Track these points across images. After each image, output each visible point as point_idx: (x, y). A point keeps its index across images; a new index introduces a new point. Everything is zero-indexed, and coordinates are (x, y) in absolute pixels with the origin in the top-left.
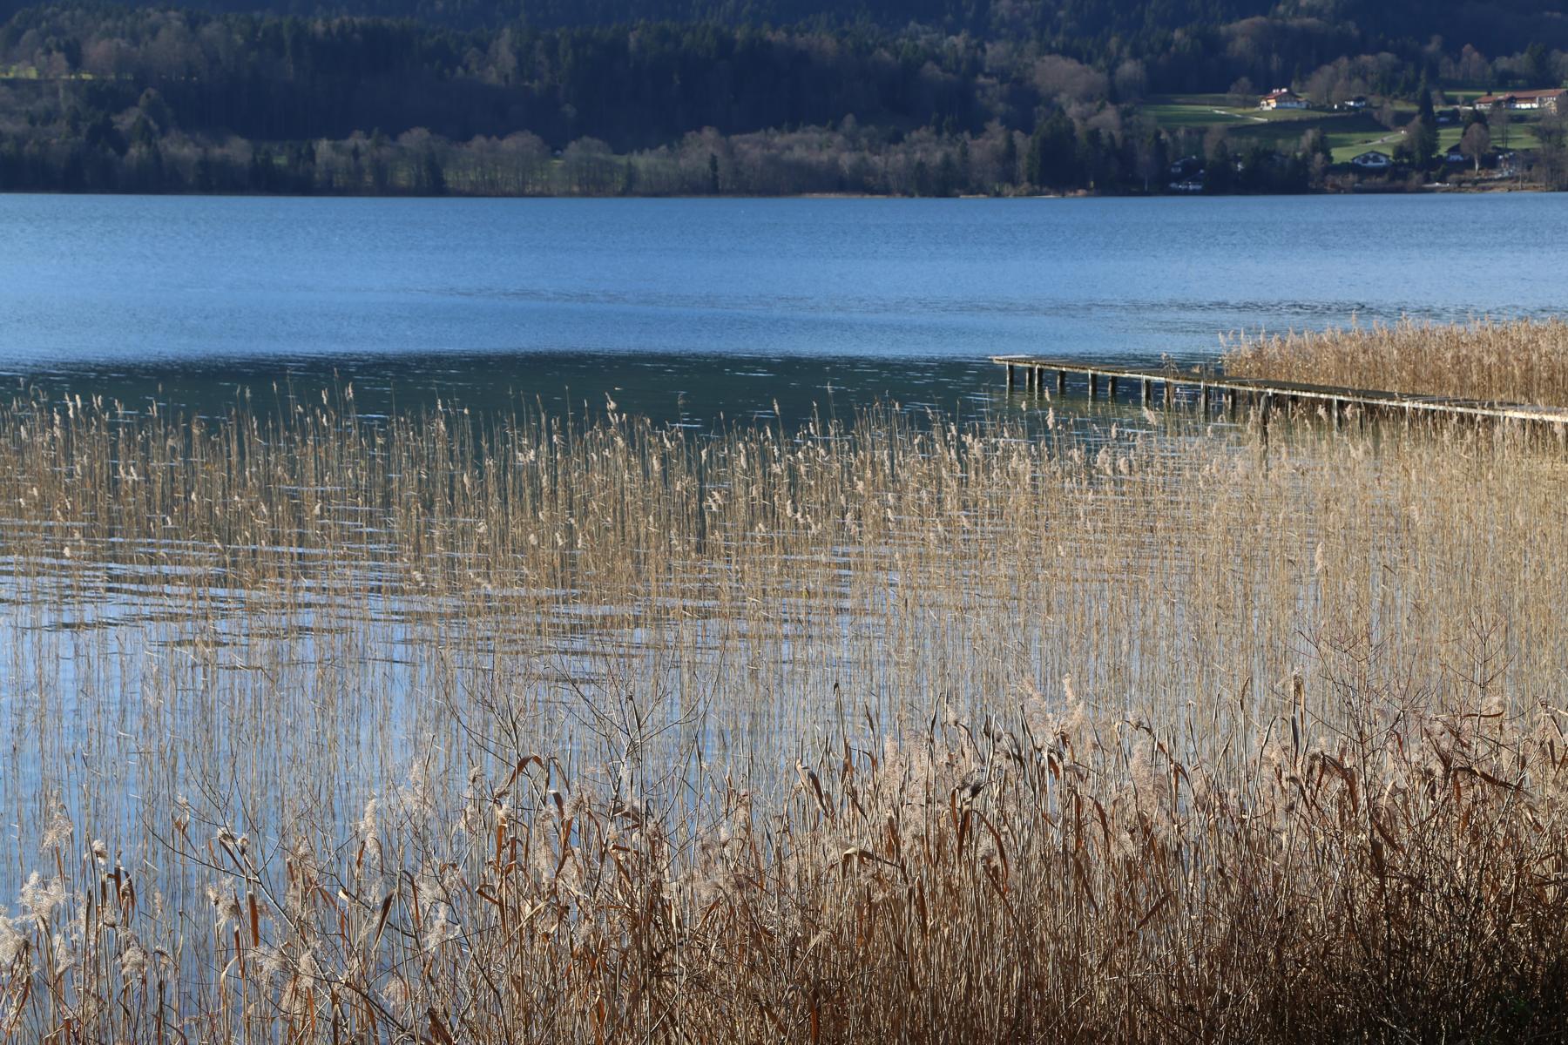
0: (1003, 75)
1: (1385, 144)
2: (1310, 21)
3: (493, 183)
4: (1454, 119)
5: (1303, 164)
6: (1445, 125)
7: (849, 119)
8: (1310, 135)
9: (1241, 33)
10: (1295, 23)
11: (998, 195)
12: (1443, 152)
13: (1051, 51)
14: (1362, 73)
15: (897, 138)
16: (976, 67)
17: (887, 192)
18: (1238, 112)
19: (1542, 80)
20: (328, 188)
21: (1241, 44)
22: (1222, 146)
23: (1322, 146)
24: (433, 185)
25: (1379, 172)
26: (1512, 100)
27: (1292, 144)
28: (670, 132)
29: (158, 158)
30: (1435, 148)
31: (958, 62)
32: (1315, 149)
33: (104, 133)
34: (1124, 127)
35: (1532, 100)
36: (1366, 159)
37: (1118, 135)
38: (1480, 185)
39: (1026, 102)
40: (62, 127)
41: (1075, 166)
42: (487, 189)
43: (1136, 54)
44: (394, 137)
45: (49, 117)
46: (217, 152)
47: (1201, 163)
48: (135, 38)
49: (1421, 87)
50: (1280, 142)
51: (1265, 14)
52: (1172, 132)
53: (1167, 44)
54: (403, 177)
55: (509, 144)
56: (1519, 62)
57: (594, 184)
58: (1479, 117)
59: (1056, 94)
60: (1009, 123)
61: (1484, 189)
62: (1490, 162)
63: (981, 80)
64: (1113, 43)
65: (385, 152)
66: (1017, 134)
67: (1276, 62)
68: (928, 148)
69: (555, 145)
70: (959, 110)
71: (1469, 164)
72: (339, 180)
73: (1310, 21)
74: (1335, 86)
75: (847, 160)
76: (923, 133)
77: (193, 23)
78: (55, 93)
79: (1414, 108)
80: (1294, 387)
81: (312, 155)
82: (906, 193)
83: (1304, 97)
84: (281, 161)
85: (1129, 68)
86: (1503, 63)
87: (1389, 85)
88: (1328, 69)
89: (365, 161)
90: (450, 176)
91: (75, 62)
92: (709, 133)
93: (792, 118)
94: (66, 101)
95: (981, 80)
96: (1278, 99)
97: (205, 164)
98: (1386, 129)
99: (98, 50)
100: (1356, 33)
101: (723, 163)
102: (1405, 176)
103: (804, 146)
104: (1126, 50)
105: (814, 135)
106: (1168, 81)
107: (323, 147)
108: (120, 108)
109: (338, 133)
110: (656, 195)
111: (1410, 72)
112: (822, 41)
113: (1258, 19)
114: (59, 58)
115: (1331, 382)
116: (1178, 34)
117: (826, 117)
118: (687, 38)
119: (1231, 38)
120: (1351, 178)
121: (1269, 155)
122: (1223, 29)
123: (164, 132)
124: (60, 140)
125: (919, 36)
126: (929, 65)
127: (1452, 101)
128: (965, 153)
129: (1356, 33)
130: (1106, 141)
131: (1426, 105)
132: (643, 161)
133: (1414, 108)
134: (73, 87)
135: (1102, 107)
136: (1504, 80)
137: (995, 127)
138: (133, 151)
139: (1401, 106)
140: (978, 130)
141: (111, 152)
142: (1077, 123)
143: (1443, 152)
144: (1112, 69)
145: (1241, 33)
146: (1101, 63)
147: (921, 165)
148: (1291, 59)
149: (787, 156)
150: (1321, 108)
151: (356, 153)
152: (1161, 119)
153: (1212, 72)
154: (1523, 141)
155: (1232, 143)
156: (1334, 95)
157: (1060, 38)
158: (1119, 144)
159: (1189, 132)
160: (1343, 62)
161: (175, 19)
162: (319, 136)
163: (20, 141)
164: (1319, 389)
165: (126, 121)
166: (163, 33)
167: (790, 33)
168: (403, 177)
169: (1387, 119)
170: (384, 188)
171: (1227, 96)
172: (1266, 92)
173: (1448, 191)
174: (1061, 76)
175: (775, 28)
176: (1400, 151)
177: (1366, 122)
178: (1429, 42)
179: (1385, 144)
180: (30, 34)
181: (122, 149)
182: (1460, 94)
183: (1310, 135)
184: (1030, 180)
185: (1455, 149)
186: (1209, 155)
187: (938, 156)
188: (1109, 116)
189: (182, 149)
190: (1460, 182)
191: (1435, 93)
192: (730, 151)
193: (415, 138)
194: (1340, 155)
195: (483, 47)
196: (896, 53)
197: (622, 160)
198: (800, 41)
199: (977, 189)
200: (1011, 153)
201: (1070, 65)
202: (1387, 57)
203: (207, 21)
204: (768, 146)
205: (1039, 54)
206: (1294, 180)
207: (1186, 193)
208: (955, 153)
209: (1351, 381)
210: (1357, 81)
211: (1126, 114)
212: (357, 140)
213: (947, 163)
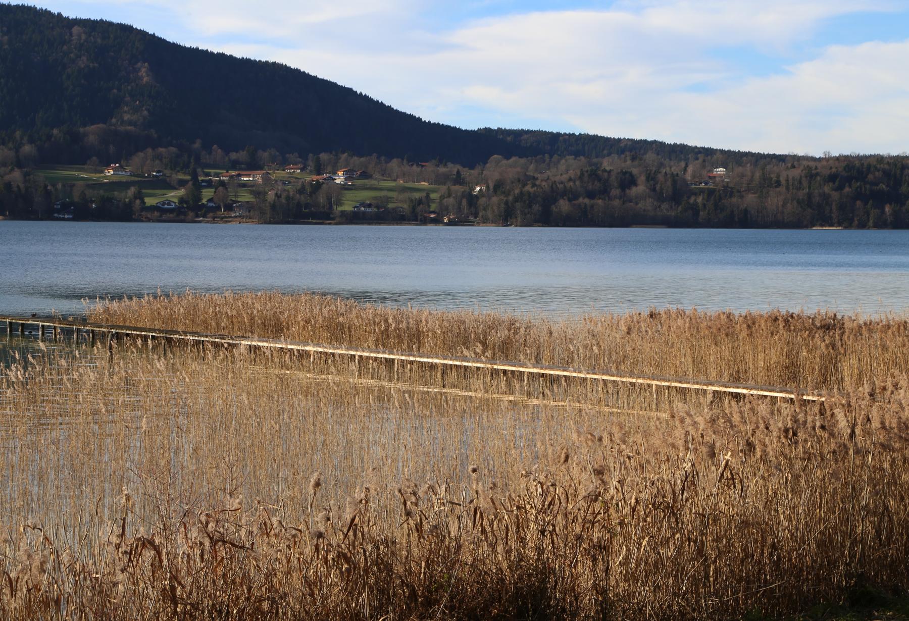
1: (174, 196)
2: (129, 128)
4: (209, 184)
5: (129, 206)
8: (132, 190)
9: (92, 132)
10: (122, 128)
12: (204, 201)
14: (159, 157)
18: (94, 176)
19: (253, 165)
21: (92, 139)
23: (140, 196)
25: (171, 211)
26: (239, 175)
27: (123, 195)
30: (200, 199)
32: (136, 198)
38: (225, 220)
43: (31, 141)
49: (192, 166)
50: (116, 193)
51: (105, 123)
52: (54, 185)
56: (241, 155)
58: (222, 183)
62: (229, 208)
64: (18, 134)
67: (112, 148)
71: (218, 208)
73: (129, 128)
74: (145, 163)
79: (188, 177)
83: (128, 169)
85: (27, 149)
86: (234, 156)
87: (174, 165)
88: (141, 154)
96: (114, 169)
98: (173, 188)
102: (185, 214)
104: (26, 139)
106: (51, 157)
113: (101, 125)
116: (55, 131)
120: (156, 214)
122: (81, 130)
127: (208, 175)
130: (15, 189)
131: (195, 176)
133: (188, 177)
135: (12, 170)
136: (234, 165)
139: (181, 176)
143: (204, 201)
144: (17, 149)
145: (92, 132)
146: (10, 145)
148: (120, 148)
150: (138, 176)
153: (77, 154)
154: (245, 197)
155: (89, 193)
158: (23, 191)
159: (64, 186)
160: (149, 150)
172: (107, 165)
176: (182, 200)
177: (165, 184)
178: (195, 143)
179: (174, 196)
182: (212, 171)
183: (132, 190)
185: (210, 200)
186: (76, 199)
188: (16, 176)
191: (199, 170)
194: (150, 201)
202: (173, 149)
206: (124, 213)
207: (64, 219)
210: (157, 162)
211: (26, 175)
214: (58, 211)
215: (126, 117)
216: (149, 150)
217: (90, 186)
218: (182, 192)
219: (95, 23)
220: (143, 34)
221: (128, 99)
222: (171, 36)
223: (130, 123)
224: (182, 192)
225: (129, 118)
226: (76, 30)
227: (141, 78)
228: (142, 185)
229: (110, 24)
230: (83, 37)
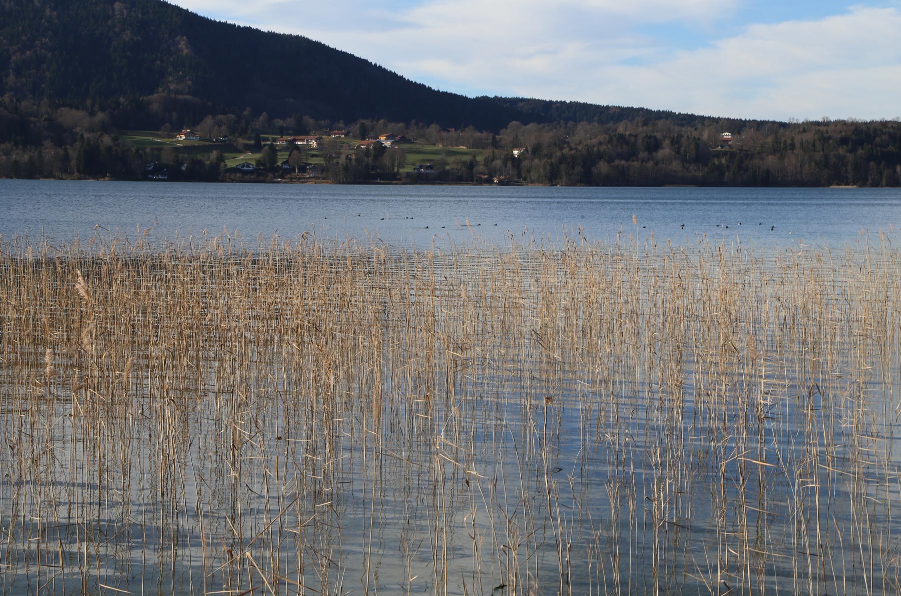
23: (221, 159)
25: (251, 172)
35: (303, 140)
36: (243, 166)
39: (61, 135)
61: (303, 182)
62: (303, 169)
96: (186, 134)
120: (239, 175)
128: (40, 156)
147: (16, 162)
159: (152, 149)
171: (159, 133)
172: (180, 132)
173: (286, 182)
176: (259, 163)
184: (79, 171)
187: (26, 157)
190: (292, 178)
194: (230, 164)
199: (49, 175)
207: (159, 180)
221: (170, 69)
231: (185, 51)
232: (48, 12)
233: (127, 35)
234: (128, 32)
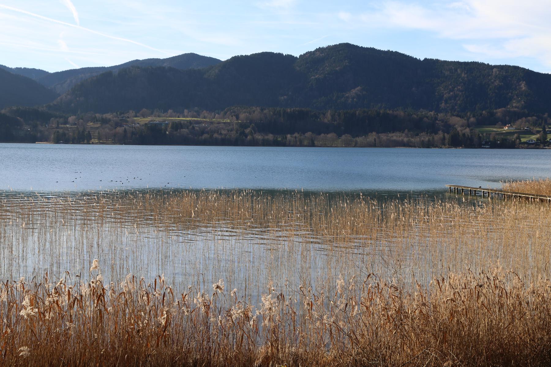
0: (442, 121)
1: (534, 137)
2: (515, 109)
3: (325, 144)
6: (549, 133)
7: (406, 131)
8: (516, 135)
9: (499, 112)
10: (512, 110)
11: (441, 148)
12: (548, 140)
13: (454, 116)
14: (528, 121)
15: (417, 135)
16: (436, 119)
17: (415, 147)
18: (499, 130)
20: (290, 145)
22: (494, 138)
23: (519, 138)
24: (312, 144)
25: (533, 144)
27: (511, 137)
28: (365, 132)
29: (254, 138)
30: (546, 139)
31: (432, 118)
32: (517, 139)
33: (243, 134)
34: (471, 133)
37: (469, 134)
39: (448, 127)
40: (234, 132)
41: (458, 142)
42: (325, 146)
43: (474, 116)
44: (304, 134)
45: (232, 130)
46: (266, 137)
47: (490, 141)
48: (250, 114)
49: (543, 125)
50: (508, 137)
51: (505, 107)
52: (482, 134)
53: (481, 114)
54: (306, 143)
55: (329, 135)
57: (348, 144)
59: (455, 125)
60: (444, 132)
63: (437, 122)
64: (469, 114)
65: (302, 137)
66: (446, 134)
67: (507, 118)
68: (425, 137)
69: (339, 135)
70: (432, 128)
72: (292, 143)
73: (515, 109)
74: (522, 124)
75: (406, 140)
76: (424, 133)
77: (262, 110)
78: (233, 125)
79: (541, 129)
80: (520, 194)
81: (286, 138)
82: (419, 147)
83: (514, 126)
84: (280, 139)
85: (472, 119)
87: (535, 124)
88: (520, 120)
89: (297, 139)
90: (316, 143)
91: (238, 118)
92: (374, 133)
93: (394, 130)
94: (235, 127)
95: (437, 122)
97: (263, 140)
98: (534, 134)
99: (242, 116)
100: (527, 112)
101: (377, 140)
102: (539, 145)
103: (396, 136)
104: (472, 115)
105: (398, 134)
106: (481, 122)
107: (289, 136)
108: (246, 128)
109: (292, 133)
110: (362, 147)
111: (540, 121)
112: (400, 113)
113: (503, 109)
114: (234, 117)
115: (529, 193)
116: (484, 112)
117: (401, 130)
118: (370, 112)
119: (496, 113)
120: (526, 145)
121: (506, 140)
122: (495, 111)
123: (255, 133)
124: (233, 135)
125: (423, 112)
126: (425, 119)
128: (433, 138)
129: (527, 112)
130: (467, 136)
131: (544, 129)
132: (359, 139)
133: (541, 129)
134: (237, 124)
135: (466, 128)
137: (440, 132)
138: (249, 137)
139: (538, 129)
140: (436, 133)
141: (244, 137)
142: (460, 132)
143: (548, 140)
144: (468, 120)
145: (499, 112)
146: (466, 118)
147: (423, 141)
149: (392, 138)
151: (296, 137)
152: (480, 131)
153: (492, 121)
155: (497, 137)
156: (522, 126)
157: (456, 112)
158: (470, 136)
159: (486, 134)
160: (524, 119)
161: (258, 109)
162: (288, 134)
163: (226, 135)
164: (526, 194)
165: (247, 131)
166: (256, 112)
167: (393, 111)
168: (306, 143)
169: (534, 132)
170: (301, 145)
172: (505, 125)
174: (457, 121)
175: (390, 110)
176: (538, 139)
178: (545, 114)
179: (534, 137)
180: (229, 112)
181: (246, 137)
183: (516, 135)
184: (449, 144)
186: (491, 140)
187: (427, 139)
188: (467, 131)
189: (259, 137)
191: (546, 126)
192: (379, 137)
193: (308, 134)
194: (523, 140)
195: (324, 114)
196: (417, 116)
197: (354, 139)
198: (395, 113)
199: (436, 146)
200: (444, 138)
201: (458, 119)
202: (535, 118)
203: (265, 109)
204: (387, 136)
205: (451, 116)
206: (512, 145)
207: (486, 148)
208: (431, 138)
209: (533, 192)
210: (527, 123)
212: (296, 135)
213: (429, 140)
214: (484, 145)
215: (514, 105)
216: (524, 119)
217: (497, 134)
218: (538, 136)
219: (503, 66)
220: (524, 69)
221: (515, 97)
222: (536, 70)
223: (516, 107)
224: (538, 136)
225: (515, 105)
226: (494, 70)
227: (522, 88)
228: (520, 133)
229: (510, 66)
230: (498, 72)
231: (524, 88)
232: (463, 75)
233: (497, 83)
234: (497, 81)
